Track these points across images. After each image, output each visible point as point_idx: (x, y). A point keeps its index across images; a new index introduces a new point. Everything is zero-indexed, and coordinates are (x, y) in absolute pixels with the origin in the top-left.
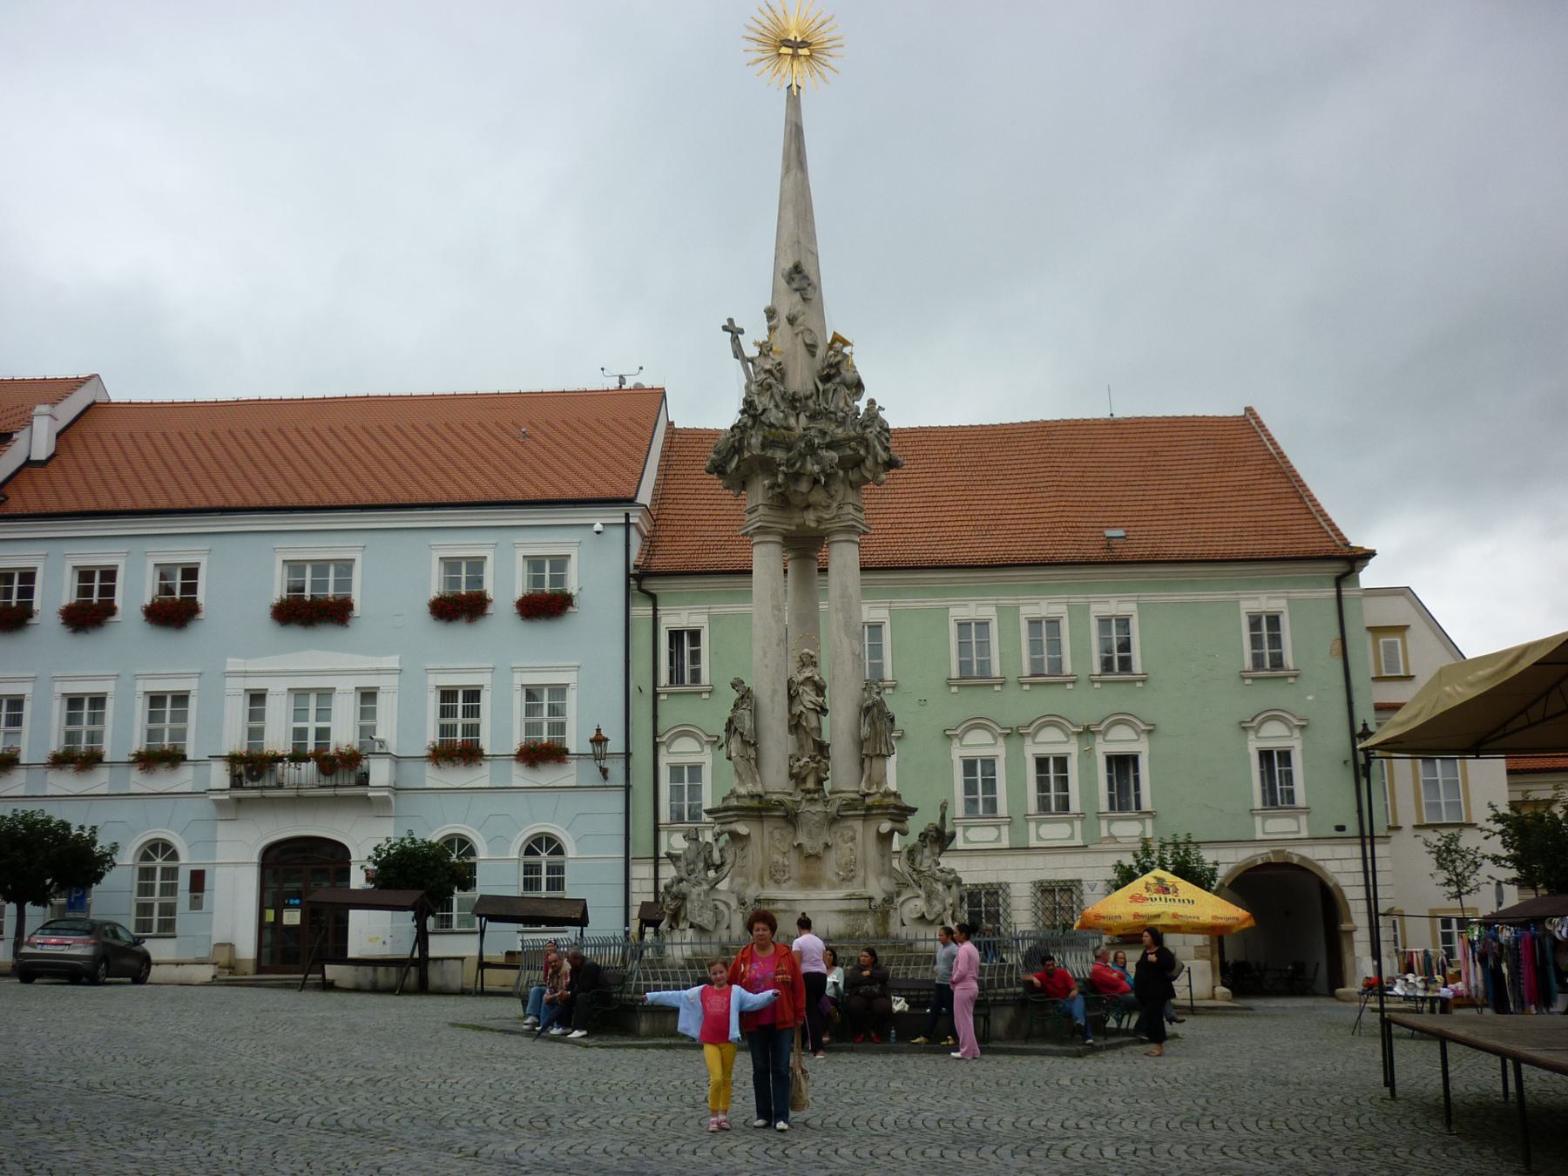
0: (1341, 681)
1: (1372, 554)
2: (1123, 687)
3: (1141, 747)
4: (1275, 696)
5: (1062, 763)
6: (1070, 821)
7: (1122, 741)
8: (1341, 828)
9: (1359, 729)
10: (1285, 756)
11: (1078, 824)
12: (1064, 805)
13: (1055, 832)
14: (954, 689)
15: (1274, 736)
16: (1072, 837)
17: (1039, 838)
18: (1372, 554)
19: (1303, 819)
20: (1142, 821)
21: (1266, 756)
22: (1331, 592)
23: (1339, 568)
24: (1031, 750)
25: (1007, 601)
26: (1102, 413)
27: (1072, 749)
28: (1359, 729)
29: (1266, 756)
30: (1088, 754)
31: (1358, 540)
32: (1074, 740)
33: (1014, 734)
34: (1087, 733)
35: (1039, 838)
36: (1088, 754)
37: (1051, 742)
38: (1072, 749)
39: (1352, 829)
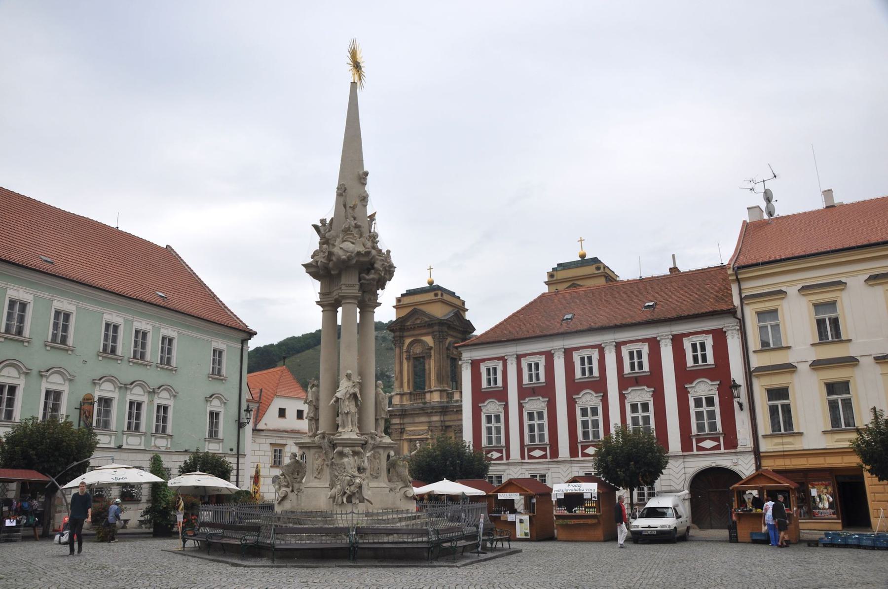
0: (238, 386)
1: (255, 333)
2: (168, 372)
3: (170, 402)
4: (217, 387)
5: (139, 405)
6: (140, 436)
7: (163, 398)
8: (231, 450)
9: (244, 406)
10: (217, 414)
11: (143, 438)
12: (137, 427)
13: (133, 441)
14: (100, 358)
15: (215, 406)
16: (140, 444)
17: (127, 444)
18: (255, 333)
20: (167, 439)
21: (212, 413)
22: (240, 346)
23: (244, 336)
24: (129, 397)
25: (129, 317)
26: (113, 225)
27: (145, 399)
28: (244, 406)
29: (212, 413)
30: (151, 401)
31: (252, 327)
32: (146, 394)
33: (125, 387)
34: (153, 392)
35: (127, 444)
36: (151, 401)
37: (137, 394)
38: (145, 399)
39: (235, 451)
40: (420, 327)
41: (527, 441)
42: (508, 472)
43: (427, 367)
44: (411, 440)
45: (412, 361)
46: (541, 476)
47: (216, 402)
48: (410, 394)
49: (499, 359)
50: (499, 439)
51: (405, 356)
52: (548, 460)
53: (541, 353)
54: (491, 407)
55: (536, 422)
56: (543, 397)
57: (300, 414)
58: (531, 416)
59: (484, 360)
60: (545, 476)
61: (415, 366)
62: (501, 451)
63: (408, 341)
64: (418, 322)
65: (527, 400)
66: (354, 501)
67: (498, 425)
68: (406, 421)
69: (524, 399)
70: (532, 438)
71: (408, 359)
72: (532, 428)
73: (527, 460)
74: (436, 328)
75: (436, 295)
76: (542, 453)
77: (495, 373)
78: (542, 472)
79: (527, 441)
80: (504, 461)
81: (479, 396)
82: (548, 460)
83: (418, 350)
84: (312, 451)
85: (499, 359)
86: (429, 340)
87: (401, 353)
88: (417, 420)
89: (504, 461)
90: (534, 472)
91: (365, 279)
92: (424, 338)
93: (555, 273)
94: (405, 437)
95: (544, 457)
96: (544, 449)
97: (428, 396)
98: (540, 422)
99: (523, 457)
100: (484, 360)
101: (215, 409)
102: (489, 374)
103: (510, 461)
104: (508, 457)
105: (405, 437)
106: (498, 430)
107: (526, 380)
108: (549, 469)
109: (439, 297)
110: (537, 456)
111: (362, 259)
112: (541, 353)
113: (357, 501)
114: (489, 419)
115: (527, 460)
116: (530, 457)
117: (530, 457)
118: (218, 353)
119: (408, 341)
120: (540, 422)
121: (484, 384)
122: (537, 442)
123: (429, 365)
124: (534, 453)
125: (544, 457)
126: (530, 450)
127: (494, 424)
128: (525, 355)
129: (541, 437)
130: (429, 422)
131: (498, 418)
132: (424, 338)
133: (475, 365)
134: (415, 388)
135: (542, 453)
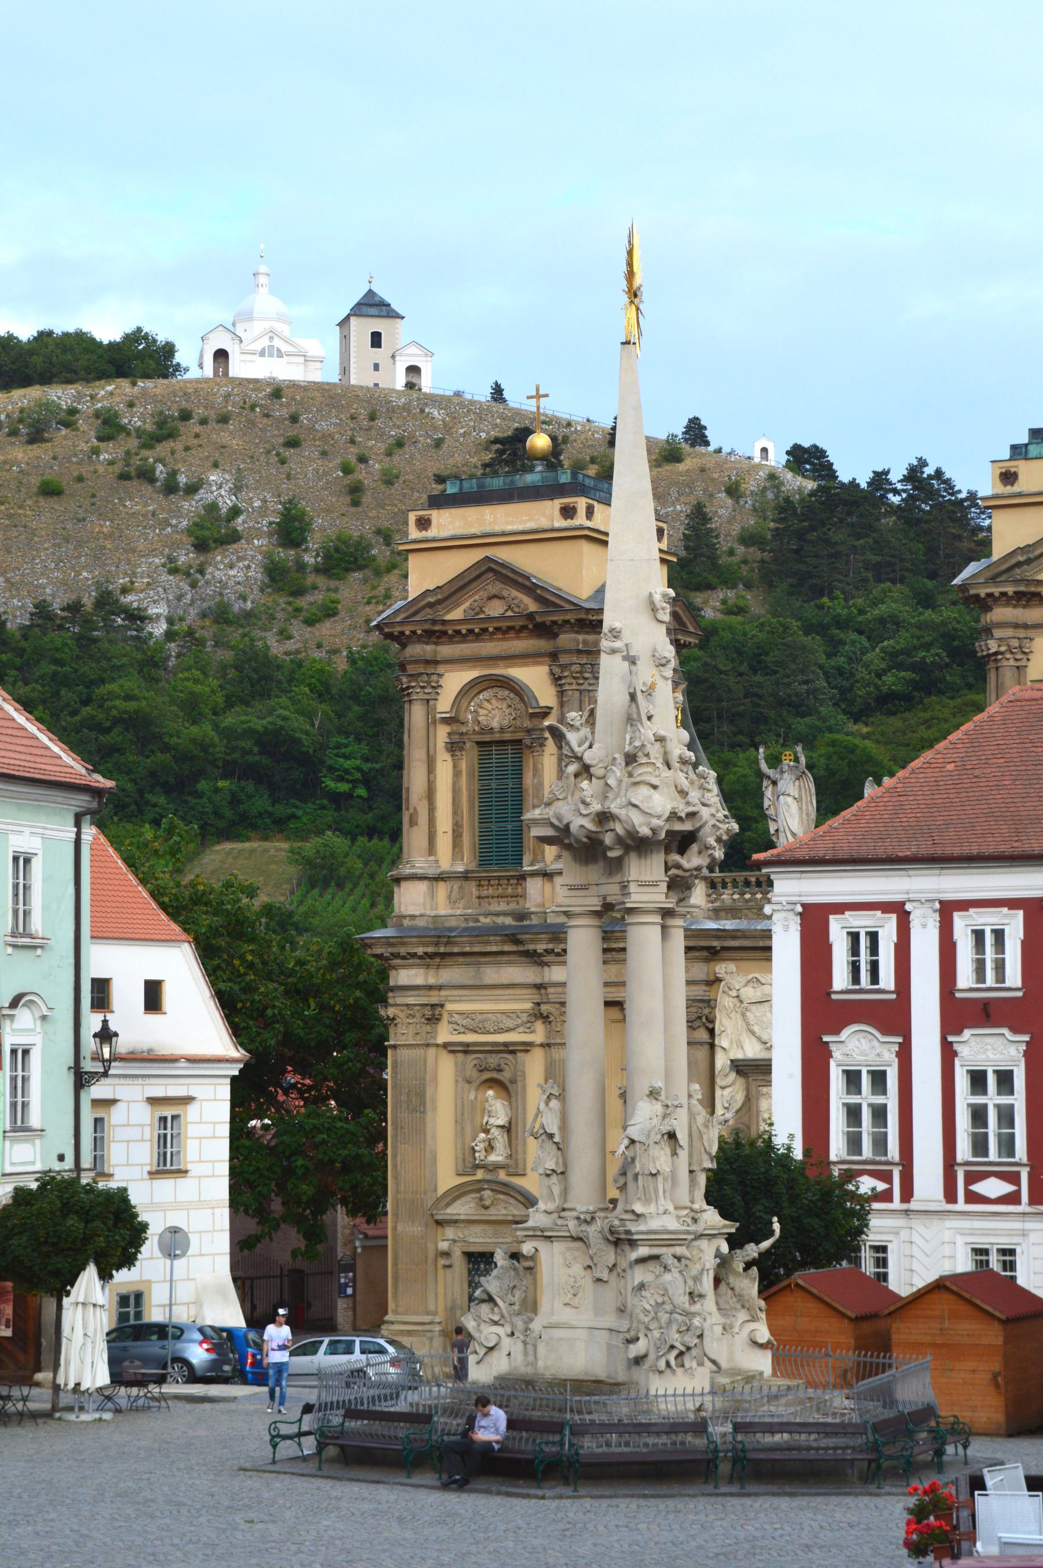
19: (38, 1142)
40: (505, 630)
41: (963, 1150)
42: (904, 1234)
43: (528, 780)
44: (466, 1049)
45: (468, 760)
46: (1003, 1252)
47: (24, 1017)
48: (465, 876)
49: (886, 907)
50: (880, 1143)
51: (442, 734)
52: (1024, 1207)
53: (1012, 904)
54: (857, 1047)
55: (992, 1099)
56: (1015, 1030)
57: (153, 996)
58: (978, 1080)
59: (840, 908)
60: (1012, 1252)
61: (484, 772)
62: (886, 1177)
63: (454, 681)
64: (495, 609)
65: (967, 1033)
66: (687, 1365)
67: (879, 1100)
68: (450, 974)
69: (959, 1032)
70: (980, 1145)
71: (454, 747)
72: (979, 1115)
73: (961, 1205)
74: (566, 639)
75: (568, 512)
76: (1007, 1188)
77: (874, 949)
78: (1006, 1242)
79: (963, 1150)
80: (896, 1204)
81: (823, 1013)
82: (1024, 1207)
83: (494, 714)
84: (558, 1247)
85: (886, 907)
86: (535, 678)
87: (432, 722)
88: (492, 974)
89: (896, 1204)
90: (982, 1241)
91: (678, 866)
92: (521, 673)
93: (1022, 467)
94: (444, 1034)
95: (1012, 1198)
96: (1013, 1178)
97: (534, 888)
98: (1005, 1100)
99: (950, 1196)
100: (840, 908)
101: (22, 1040)
102: (855, 950)
103: (913, 1205)
104: (907, 1194)
105: (444, 1034)
106: (880, 1114)
107: (965, 977)
108: (1024, 1234)
109: (580, 519)
110: (993, 1195)
111: (678, 827)
112: (1012, 904)
113: (694, 1364)
114: (852, 1079)
115: (961, 1205)
116: (973, 1198)
117: (973, 1198)
118: (22, 862)
119: (454, 681)
120: (1005, 1100)
121: (841, 979)
122: (993, 1155)
123: (537, 772)
124: (978, 1188)
125: (1012, 1198)
126: (972, 1178)
127: (867, 1098)
128: (965, 905)
129: (1007, 1145)
130: (539, 987)
131: (879, 1079)
132: (521, 673)
133: (814, 920)
134: (484, 860)
135: (1007, 1188)
